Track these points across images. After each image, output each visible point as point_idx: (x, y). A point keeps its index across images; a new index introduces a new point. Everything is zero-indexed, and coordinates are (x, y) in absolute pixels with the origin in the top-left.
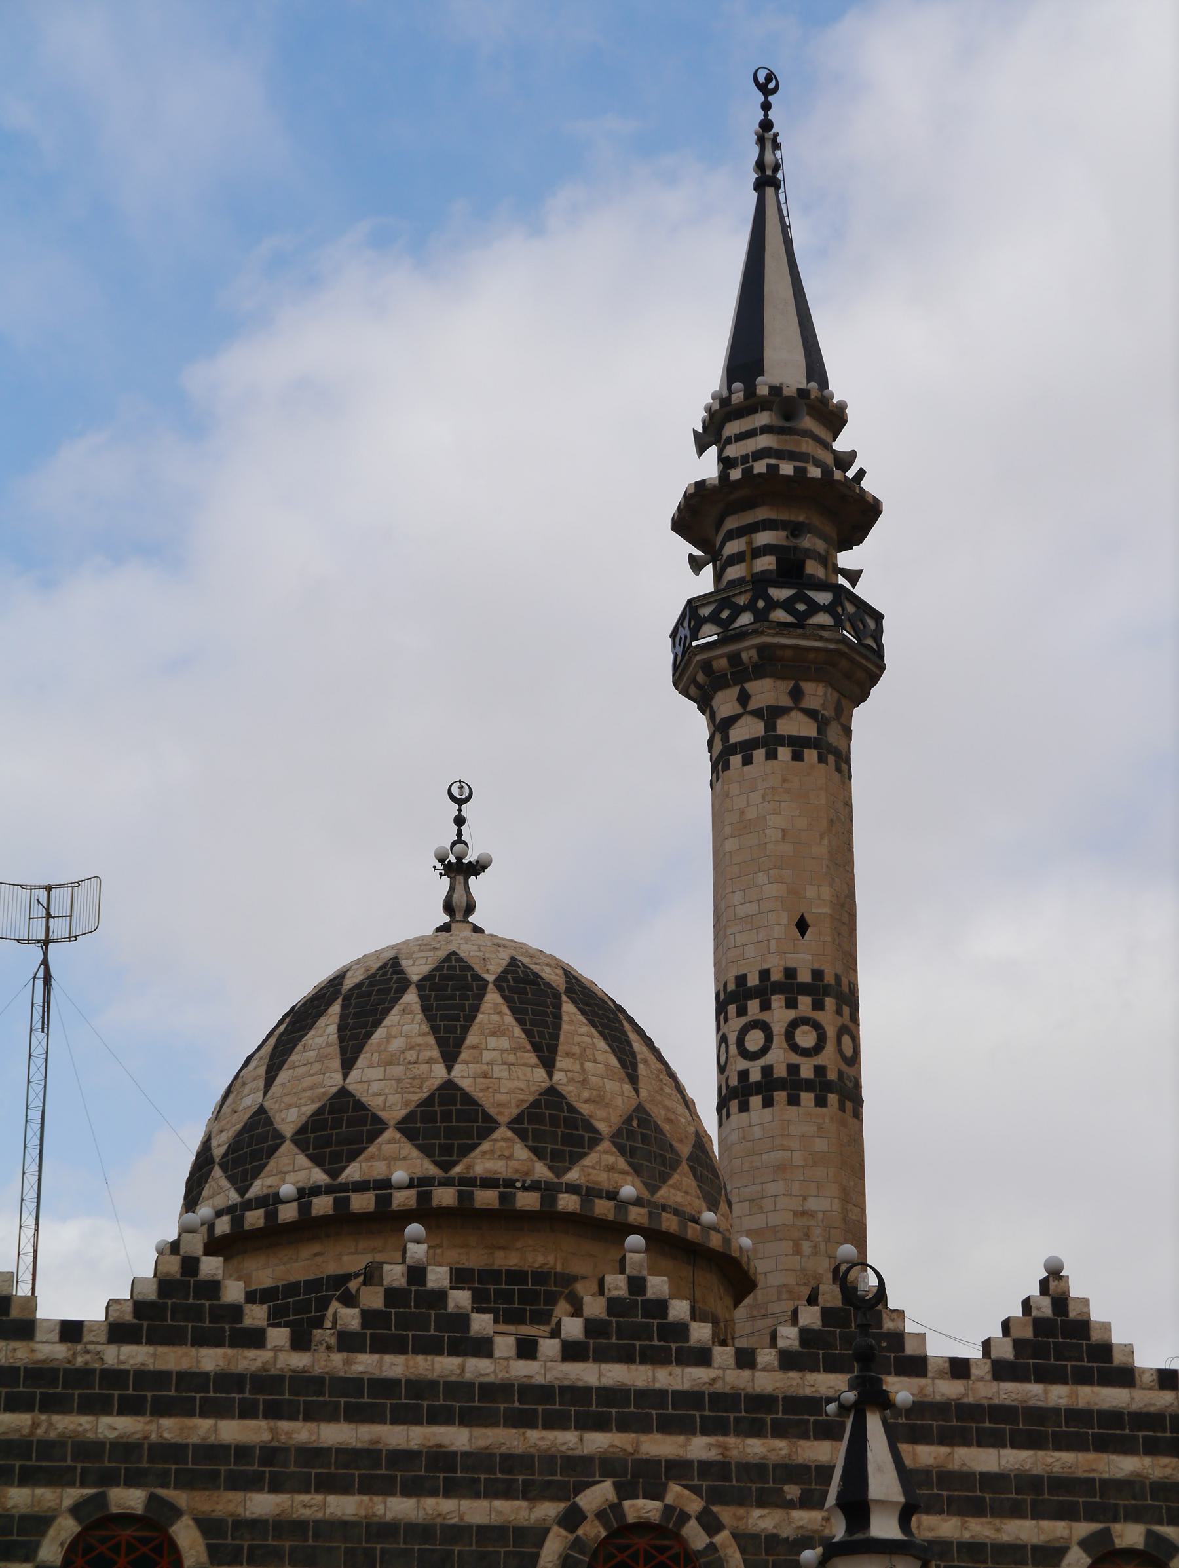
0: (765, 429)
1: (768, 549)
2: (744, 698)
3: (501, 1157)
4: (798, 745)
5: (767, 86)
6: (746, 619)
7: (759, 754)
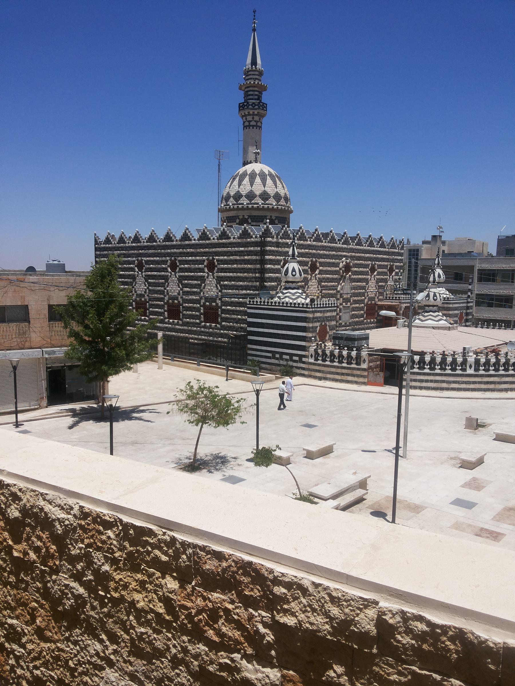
0: (257, 75)
1: (256, 95)
2: (253, 118)
3: (282, 202)
4: (253, 126)
5: (254, 12)
6: (257, 107)
7: (255, 128)
